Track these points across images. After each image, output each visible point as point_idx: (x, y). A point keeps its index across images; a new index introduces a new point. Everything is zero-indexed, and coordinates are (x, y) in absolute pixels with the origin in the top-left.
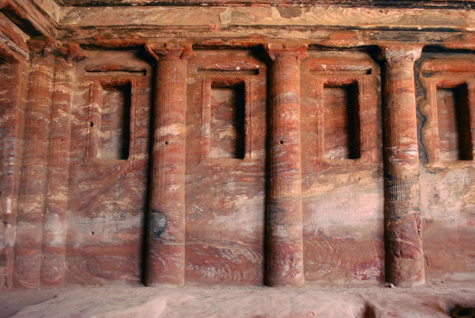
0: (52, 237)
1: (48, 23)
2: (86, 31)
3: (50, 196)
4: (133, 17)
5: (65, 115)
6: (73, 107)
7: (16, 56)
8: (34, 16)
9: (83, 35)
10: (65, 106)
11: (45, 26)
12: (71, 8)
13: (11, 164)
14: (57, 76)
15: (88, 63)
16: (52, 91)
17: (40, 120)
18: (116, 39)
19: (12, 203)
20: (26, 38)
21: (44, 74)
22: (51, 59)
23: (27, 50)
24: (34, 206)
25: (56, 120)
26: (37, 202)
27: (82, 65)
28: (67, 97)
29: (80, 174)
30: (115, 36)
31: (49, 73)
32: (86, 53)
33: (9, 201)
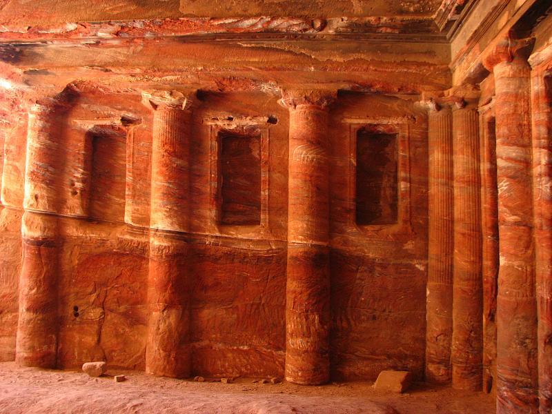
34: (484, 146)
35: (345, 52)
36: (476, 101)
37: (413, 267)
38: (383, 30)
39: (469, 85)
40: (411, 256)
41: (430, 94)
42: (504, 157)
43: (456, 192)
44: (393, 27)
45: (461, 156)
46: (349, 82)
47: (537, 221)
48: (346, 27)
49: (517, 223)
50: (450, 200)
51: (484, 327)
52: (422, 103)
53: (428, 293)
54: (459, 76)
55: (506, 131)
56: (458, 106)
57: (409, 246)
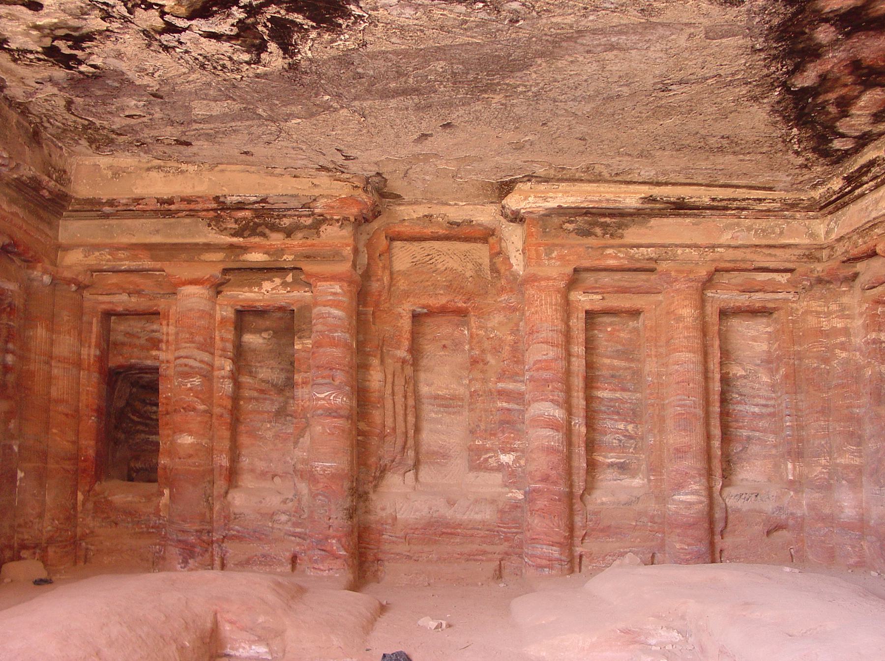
0: (841, 508)
1: (797, 252)
2: (841, 244)
3: (836, 459)
4: (870, 209)
5: (844, 355)
6: (858, 341)
7: (771, 305)
8: (769, 259)
9: (840, 249)
10: (842, 343)
11: (794, 258)
12: (829, 216)
13: (788, 424)
14: (831, 308)
15: (862, 280)
16: (828, 328)
17: (815, 369)
18: (862, 245)
19: (794, 468)
20: (783, 278)
21: (813, 311)
22: (818, 290)
23: (792, 290)
24: (818, 471)
25: (835, 363)
26: (821, 465)
27: (858, 283)
28: (846, 331)
29: (868, 429)
30: (860, 241)
31: (819, 309)
32: (860, 267)
33: (790, 466)
34: (91, 332)
35: (12, 201)
36: (86, 287)
37: (11, 448)
38: (45, 193)
39: (89, 272)
40: (12, 437)
41: (50, 268)
42: (198, 358)
43: (55, 371)
44: (50, 193)
45: (67, 337)
46: (11, 237)
47: (217, 410)
48: (29, 178)
49: (206, 411)
50: (49, 379)
51: (79, 503)
52: (36, 273)
53: (20, 475)
54: (74, 260)
55: (202, 340)
56: (73, 287)
57: (12, 426)
